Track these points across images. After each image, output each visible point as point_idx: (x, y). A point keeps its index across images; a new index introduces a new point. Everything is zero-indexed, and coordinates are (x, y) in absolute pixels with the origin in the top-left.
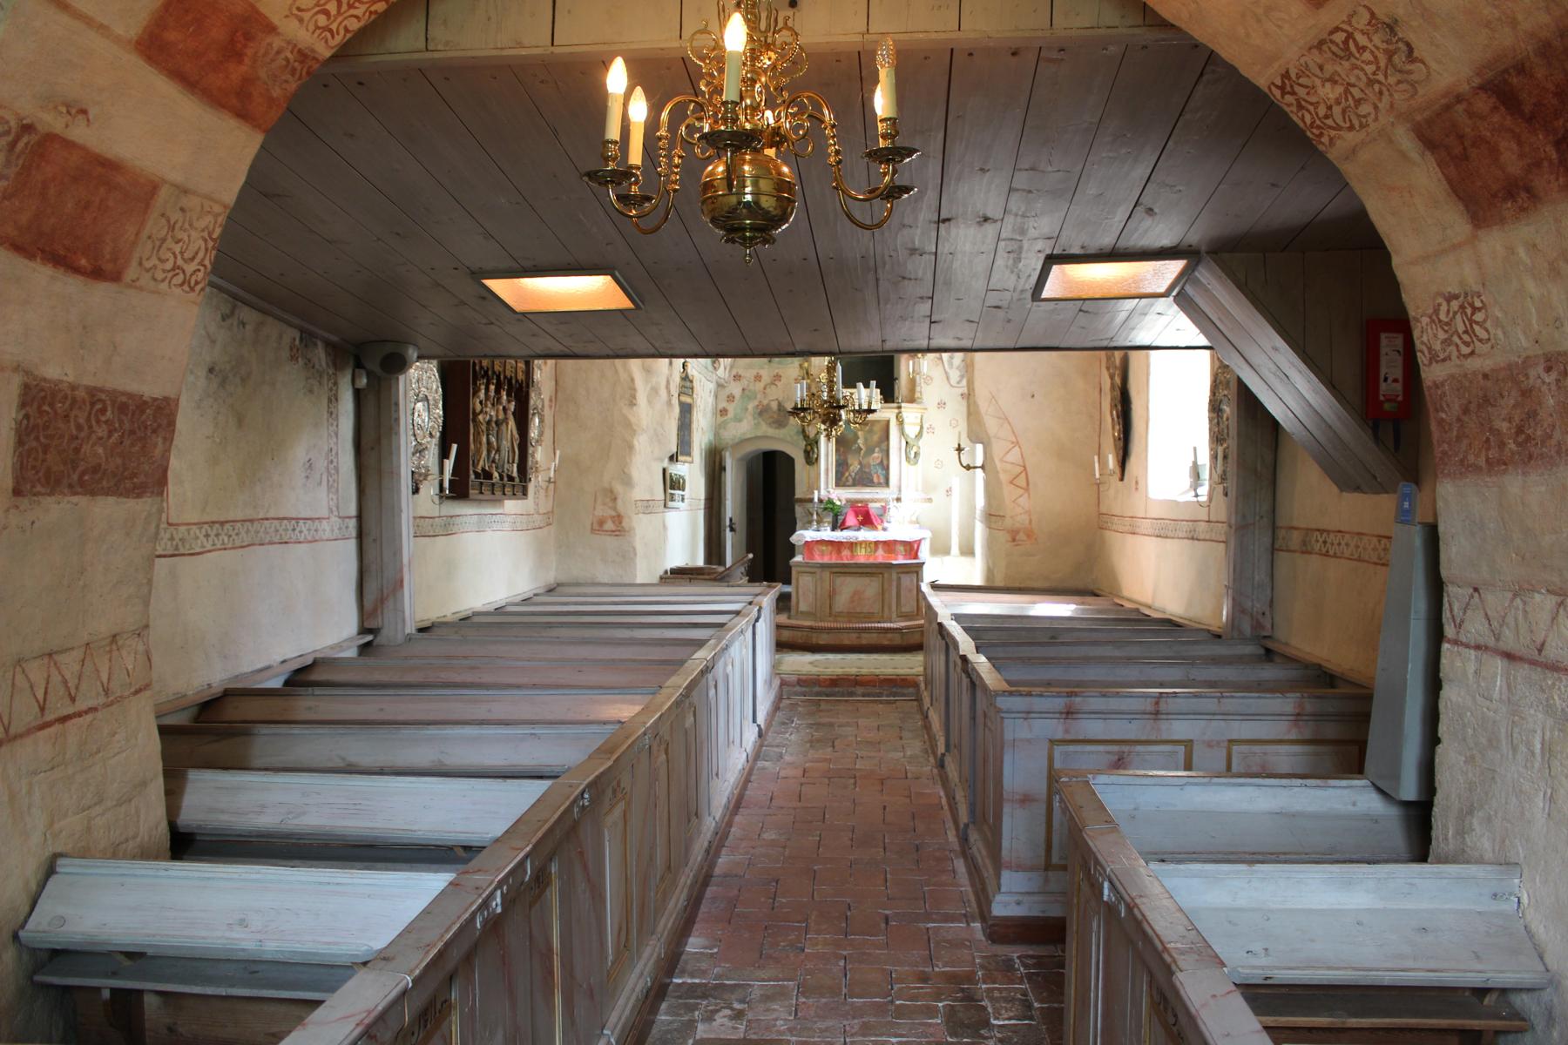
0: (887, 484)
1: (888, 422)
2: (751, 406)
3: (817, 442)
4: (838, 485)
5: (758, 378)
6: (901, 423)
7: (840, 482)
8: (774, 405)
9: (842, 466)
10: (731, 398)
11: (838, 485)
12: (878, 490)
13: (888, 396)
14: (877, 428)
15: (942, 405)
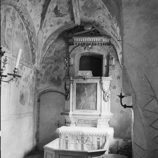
0: (96, 110)
1: (97, 83)
2: (48, 77)
3: (69, 92)
4: (77, 109)
5: (51, 67)
6: (101, 84)
7: (78, 107)
8: (56, 78)
9: (78, 101)
10: (41, 75)
11: (77, 109)
12: (92, 111)
13: (98, 73)
14: (92, 86)
15: (119, 78)
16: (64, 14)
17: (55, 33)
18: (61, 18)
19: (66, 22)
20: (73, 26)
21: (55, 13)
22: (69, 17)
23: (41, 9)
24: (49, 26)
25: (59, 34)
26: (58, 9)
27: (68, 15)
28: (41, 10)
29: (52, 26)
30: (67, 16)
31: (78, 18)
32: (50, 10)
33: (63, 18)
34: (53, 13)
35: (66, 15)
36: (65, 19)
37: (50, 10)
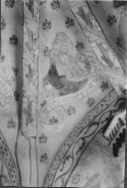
16: (79, 83)
17: (68, 139)
18: (75, 94)
19: (90, 100)
20: (112, 100)
21: (54, 85)
22: (94, 84)
23: (10, 78)
24: (48, 122)
25: (83, 138)
26: (60, 73)
27: (90, 81)
28: (14, 83)
29: (56, 121)
30: (89, 83)
31: (116, 68)
32: (30, 70)
33: (79, 93)
34: (49, 87)
35: (85, 81)
36: (85, 94)
37: (30, 70)
